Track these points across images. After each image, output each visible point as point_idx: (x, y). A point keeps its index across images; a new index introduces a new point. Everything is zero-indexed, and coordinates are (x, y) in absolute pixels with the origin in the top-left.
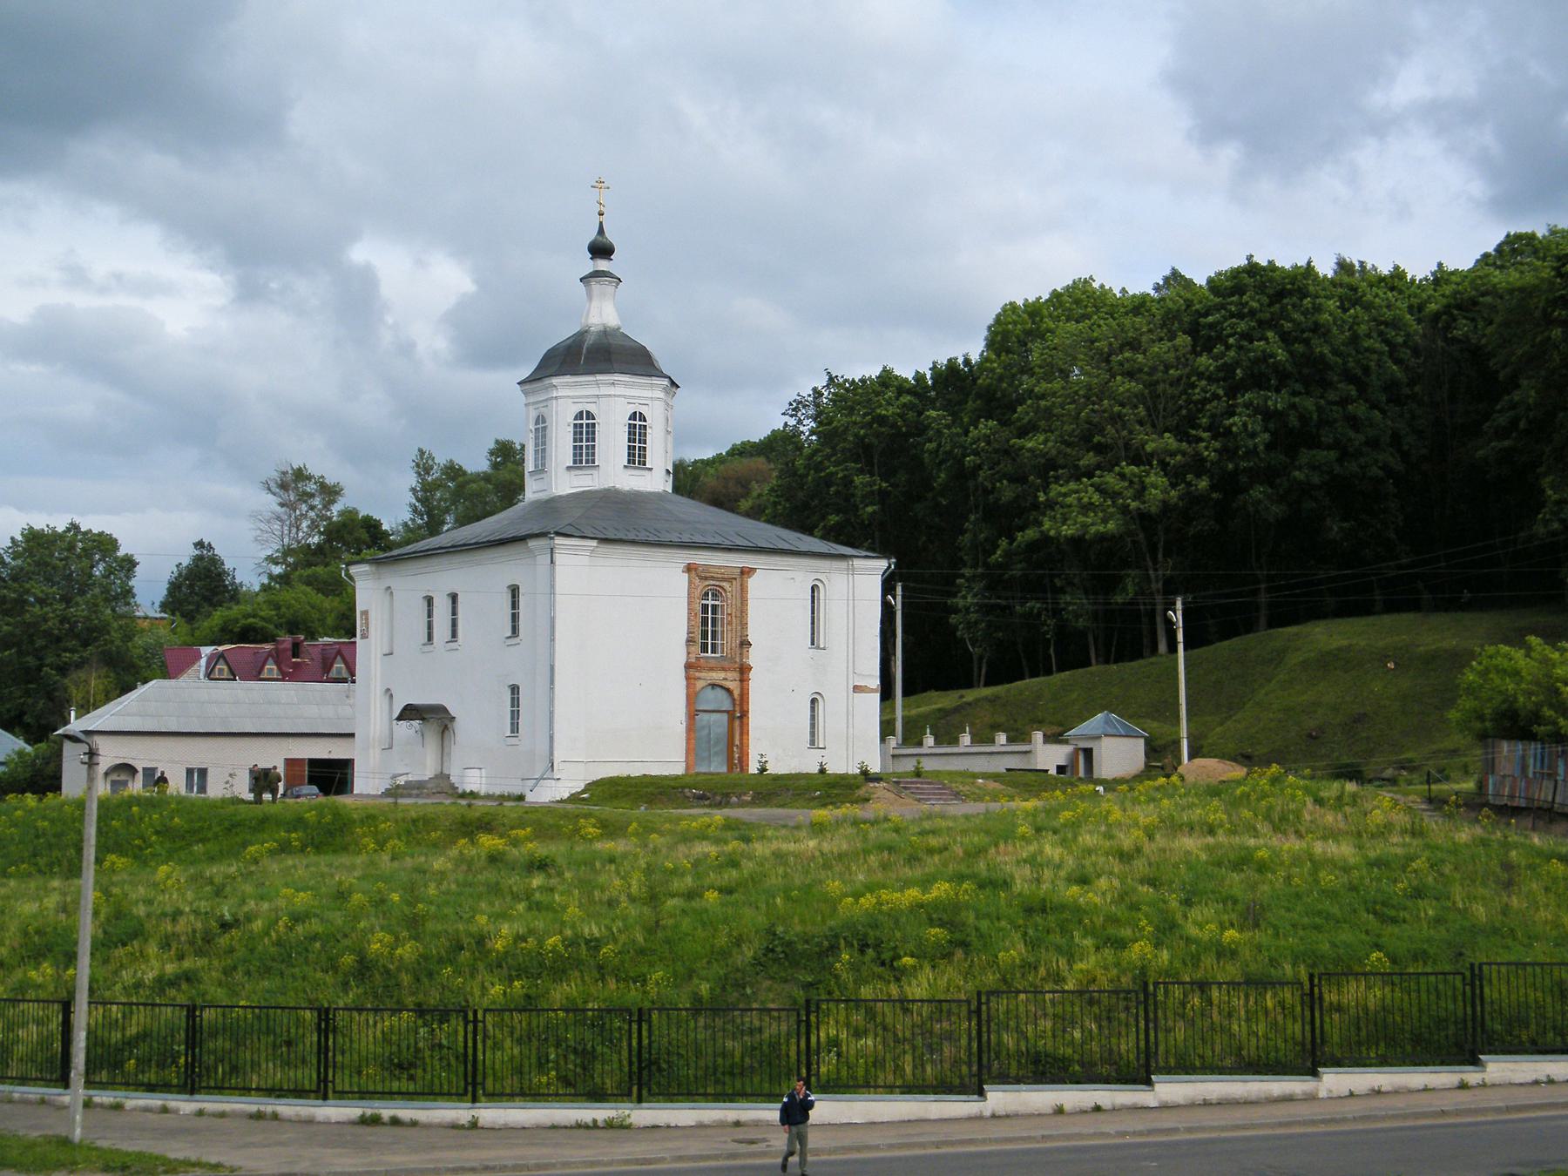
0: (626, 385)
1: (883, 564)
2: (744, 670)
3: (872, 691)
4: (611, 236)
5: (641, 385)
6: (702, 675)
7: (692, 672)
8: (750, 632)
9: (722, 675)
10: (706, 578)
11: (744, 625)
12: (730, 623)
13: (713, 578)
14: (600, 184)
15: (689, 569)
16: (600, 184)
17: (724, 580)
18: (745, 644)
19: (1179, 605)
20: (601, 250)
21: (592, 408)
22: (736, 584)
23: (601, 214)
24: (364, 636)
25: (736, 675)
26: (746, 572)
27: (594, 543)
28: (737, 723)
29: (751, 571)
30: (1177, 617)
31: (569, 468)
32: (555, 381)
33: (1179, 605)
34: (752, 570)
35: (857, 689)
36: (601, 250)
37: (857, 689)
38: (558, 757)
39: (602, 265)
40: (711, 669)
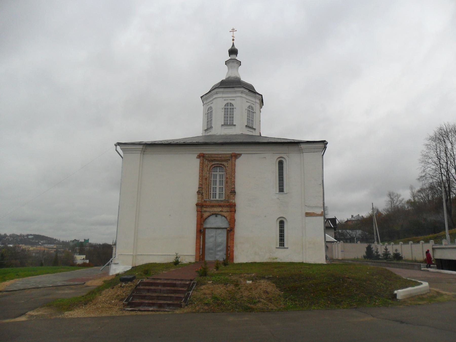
0: (223, 93)
4: (236, 47)
5: (230, 92)
6: (208, 209)
9: (220, 209)
10: (212, 161)
11: (233, 183)
13: (214, 160)
14: (233, 30)
17: (222, 161)
18: (233, 192)
20: (233, 51)
21: (212, 105)
22: (230, 162)
23: (233, 40)
27: (141, 147)
29: (236, 156)
31: (205, 130)
34: (240, 155)
35: (308, 214)
36: (233, 51)
37: (308, 214)
39: (233, 56)
40: (213, 206)
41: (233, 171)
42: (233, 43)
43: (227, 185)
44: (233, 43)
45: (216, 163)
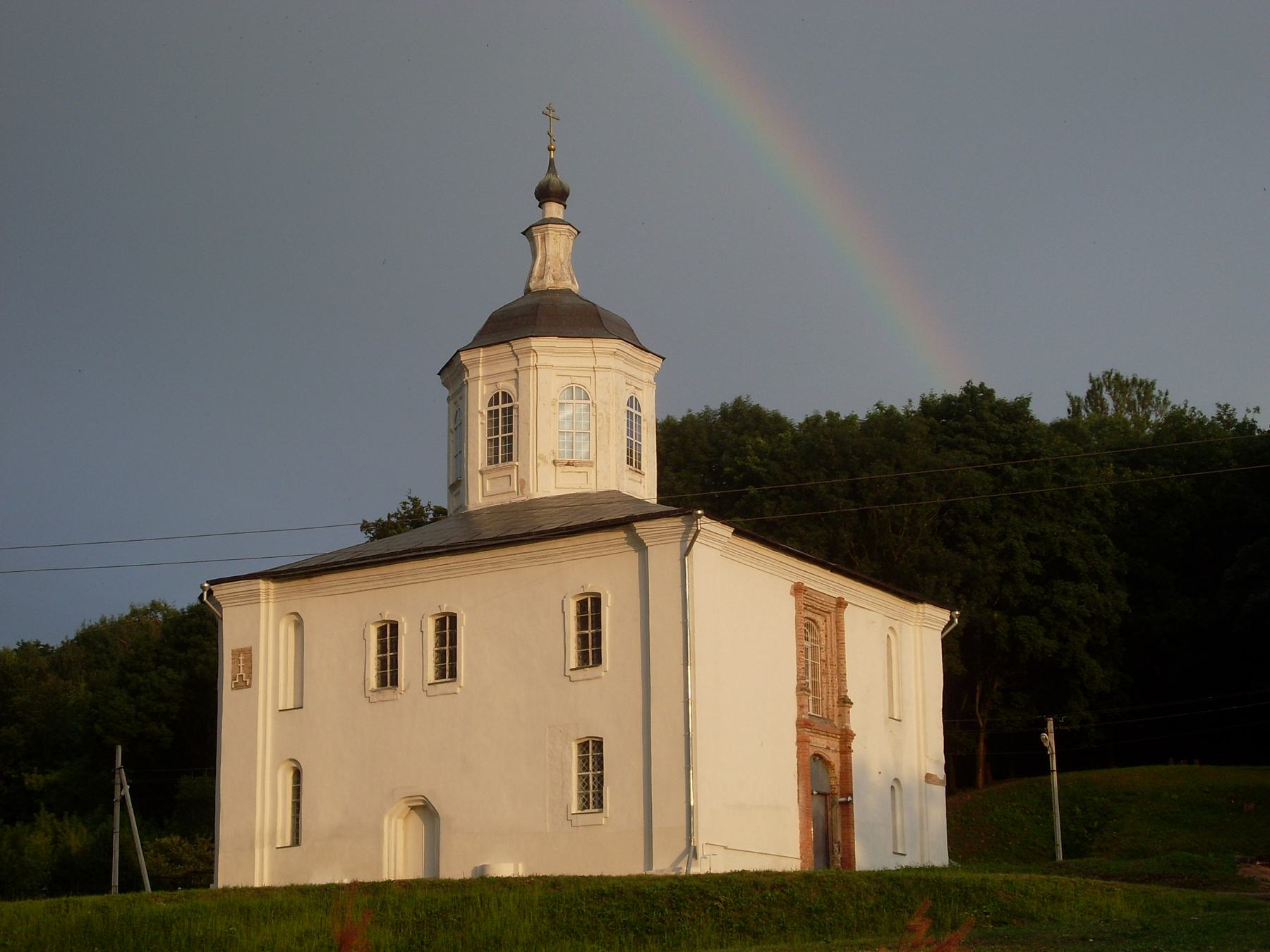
1: (943, 616)
2: (846, 737)
3: (940, 783)
4: (563, 177)
7: (807, 732)
8: (848, 687)
11: (841, 677)
12: (825, 673)
15: (798, 589)
16: (548, 112)
18: (845, 702)
19: (1050, 725)
22: (831, 620)
24: (243, 683)
25: (835, 744)
26: (841, 604)
28: (837, 812)
30: (1049, 739)
32: (536, 343)
33: (1050, 725)
38: (701, 840)
41: (840, 643)
42: (551, 162)
43: (824, 679)
44: (551, 162)
45: (810, 615)
